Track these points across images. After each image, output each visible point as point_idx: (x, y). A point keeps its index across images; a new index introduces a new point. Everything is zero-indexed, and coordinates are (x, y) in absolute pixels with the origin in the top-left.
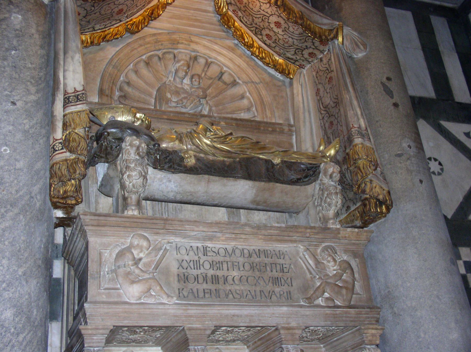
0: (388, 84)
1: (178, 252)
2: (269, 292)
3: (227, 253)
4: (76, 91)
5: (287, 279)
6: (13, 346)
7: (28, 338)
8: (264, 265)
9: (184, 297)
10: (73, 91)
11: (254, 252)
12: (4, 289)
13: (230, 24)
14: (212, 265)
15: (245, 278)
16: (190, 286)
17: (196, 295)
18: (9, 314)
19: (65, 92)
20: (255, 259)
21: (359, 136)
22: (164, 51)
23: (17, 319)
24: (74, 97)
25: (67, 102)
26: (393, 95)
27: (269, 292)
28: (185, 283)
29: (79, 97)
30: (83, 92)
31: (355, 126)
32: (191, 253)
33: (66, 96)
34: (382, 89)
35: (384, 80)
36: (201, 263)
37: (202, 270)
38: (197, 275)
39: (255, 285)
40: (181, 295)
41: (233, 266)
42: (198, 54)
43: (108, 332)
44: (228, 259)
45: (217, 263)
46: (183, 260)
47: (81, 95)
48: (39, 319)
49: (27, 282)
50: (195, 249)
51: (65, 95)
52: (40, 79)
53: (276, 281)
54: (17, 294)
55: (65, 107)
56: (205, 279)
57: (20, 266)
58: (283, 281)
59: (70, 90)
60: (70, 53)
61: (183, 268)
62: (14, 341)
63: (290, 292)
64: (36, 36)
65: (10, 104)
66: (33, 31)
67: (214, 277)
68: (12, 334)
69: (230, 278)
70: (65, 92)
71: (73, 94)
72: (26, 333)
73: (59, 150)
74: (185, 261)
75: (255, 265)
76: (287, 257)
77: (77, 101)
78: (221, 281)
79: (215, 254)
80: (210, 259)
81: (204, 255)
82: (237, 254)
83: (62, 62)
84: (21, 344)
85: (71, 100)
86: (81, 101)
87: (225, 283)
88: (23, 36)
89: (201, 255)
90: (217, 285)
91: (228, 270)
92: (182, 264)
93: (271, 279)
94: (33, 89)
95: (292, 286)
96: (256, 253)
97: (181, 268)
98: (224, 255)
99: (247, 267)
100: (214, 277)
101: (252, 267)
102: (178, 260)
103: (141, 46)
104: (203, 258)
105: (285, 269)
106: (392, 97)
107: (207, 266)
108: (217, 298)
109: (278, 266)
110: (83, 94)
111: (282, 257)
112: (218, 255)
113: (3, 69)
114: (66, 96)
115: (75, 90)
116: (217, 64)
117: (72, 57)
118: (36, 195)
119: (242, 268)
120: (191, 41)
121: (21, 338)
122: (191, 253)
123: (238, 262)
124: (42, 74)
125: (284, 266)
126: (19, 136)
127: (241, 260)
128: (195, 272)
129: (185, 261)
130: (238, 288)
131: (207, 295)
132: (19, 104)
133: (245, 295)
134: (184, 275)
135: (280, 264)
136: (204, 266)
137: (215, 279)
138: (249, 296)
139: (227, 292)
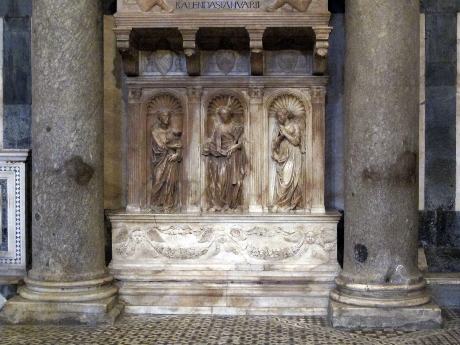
6: (72, 41)
7: (82, 36)
12: (64, 8)
18: (68, 22)
40: (178, 7)
43: (130, 32)
48: (89, 24)
54: (72, 11)
68: (71, 34)
72: (80, 32)
84: (77, 39)
108: (202, 8)
121: (76, 36)
131: (196, 6)
138: (227, 7)
139: (210, 4)
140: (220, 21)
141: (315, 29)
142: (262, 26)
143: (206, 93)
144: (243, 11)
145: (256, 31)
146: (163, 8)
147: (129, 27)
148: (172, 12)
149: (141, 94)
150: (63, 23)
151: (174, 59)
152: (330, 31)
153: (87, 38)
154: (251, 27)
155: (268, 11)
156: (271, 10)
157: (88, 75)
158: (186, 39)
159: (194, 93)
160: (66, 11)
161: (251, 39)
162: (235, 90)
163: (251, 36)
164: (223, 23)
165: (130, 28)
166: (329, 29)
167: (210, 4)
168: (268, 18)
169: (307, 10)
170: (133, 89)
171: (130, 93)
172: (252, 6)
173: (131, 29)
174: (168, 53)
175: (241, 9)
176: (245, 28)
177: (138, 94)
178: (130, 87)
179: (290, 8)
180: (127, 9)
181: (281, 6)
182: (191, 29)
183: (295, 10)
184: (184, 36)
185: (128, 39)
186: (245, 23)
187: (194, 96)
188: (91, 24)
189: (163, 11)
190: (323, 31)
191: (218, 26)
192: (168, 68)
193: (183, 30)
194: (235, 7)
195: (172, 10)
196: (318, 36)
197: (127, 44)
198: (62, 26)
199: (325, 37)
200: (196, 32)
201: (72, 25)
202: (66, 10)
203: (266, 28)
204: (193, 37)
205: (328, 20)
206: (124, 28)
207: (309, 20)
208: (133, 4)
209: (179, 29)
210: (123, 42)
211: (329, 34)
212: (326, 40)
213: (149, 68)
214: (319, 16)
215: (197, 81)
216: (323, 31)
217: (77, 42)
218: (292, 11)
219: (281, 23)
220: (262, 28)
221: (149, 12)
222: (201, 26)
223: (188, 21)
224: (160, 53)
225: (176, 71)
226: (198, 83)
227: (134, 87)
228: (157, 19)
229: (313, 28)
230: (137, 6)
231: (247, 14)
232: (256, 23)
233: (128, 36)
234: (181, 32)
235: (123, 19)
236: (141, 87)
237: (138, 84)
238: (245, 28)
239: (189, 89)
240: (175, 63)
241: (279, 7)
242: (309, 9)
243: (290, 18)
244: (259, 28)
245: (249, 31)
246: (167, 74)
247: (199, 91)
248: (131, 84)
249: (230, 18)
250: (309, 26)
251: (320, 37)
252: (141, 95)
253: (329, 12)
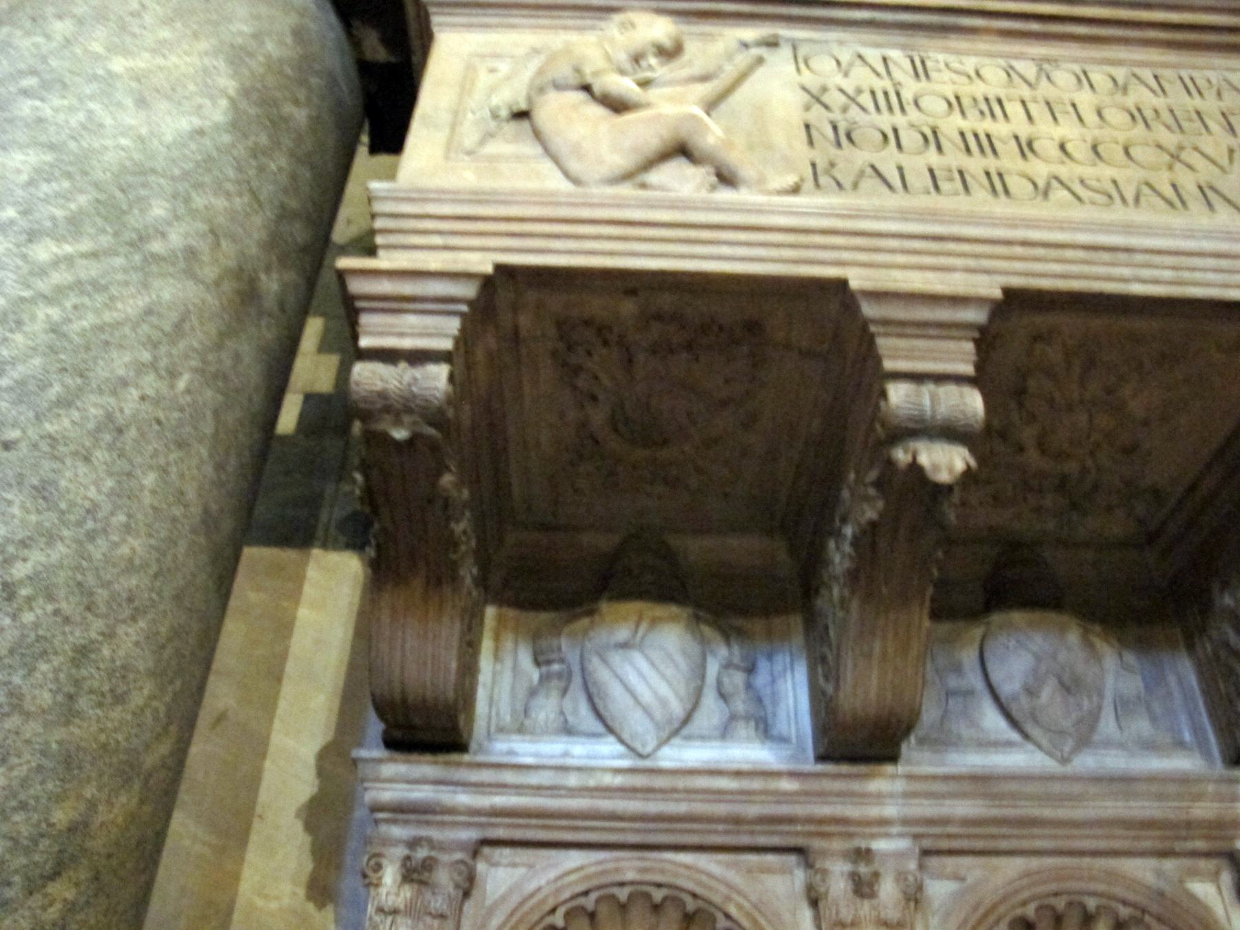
16: (861, 157)
72: (86, 246)
121: (43, 252)
128: (885, 121)
134: (835, 128)
140: (1139, 258)
143: (939, 890)
146: (726, 178)
149: (468, 886)
151: (713, 668)
153: (132, 305)
157: (37, 557)
159: (863, 887)
162: (1142, 870)
164: (1168, 274)
170: (413, 843)
171: (390, 875)
174: (673, 619)
177: (444, 878)
178: (397, 832)
185: (447, 344)
187: (865, 908)
191: (1137, 289)
192: (677, 709)
193: (878, 296)
197: (436, 380)
201: (31, 183)
204: (960, 357)
213: (546, 709)
215: (879, 797)
222: (1016, 282)
223: (917, 245)
224: (618, 623)
225: (725, 733)
226: (890, 810)
227: (423, 832)
234: (869, 310)
236: (469, 835)
237: (452, 811)
239: (824, 853)
240: (719, 684)
246: (666, 751)
247: (901, 877)
248: (402, 811)
252: (467, 894)
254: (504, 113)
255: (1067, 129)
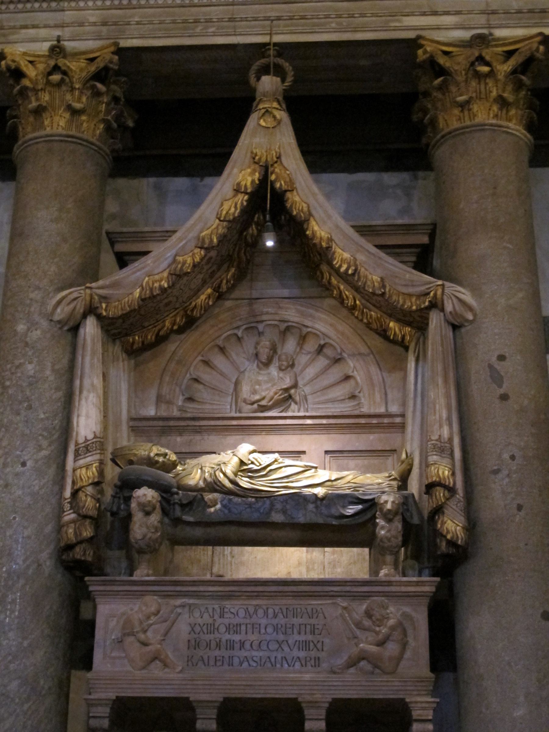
0: (498, 366)
1: (191, 616)
2: (293, 658)
3: (247, 613)
4: (86, 440)
5: (318, 642)
8: (291, 626)
9: (193, 665)
10: (84, 439)
11: (280, 611)
13: (324, 280)
14: (228, 629)
15: (266, 643)
17: (207, 663)
18: (14, 685)
19: (77, 444)
20: (281, 620)
21: (435, 453)
22: (244, 327)
23: (22, 690)
24: (84, 449)
25: (77, 454)
26: (503, 382)
27: (293, 658)
28: (195, 649)
29: (89, 448)
30: (94, 440)
31: (433, 438)
32: (206, 616)
33: (77, 447)
34: (489, 374)
35: (494, 359)
36: (216, 626)
37: (217, 635)
38: (210, 641)
39: (277, 650)
41: (253, 628)
42: (290, 324)
43: (111, 702)
44: (248, 621)
45: (234, 626)
46: (195, 624)
47: (91, 445)
48: (46, 687)
49: (33, 653)
50: (210, 610)
51: (76, 446)
52: (54, 428)
53: (305, 645)
55: (75, 461)
56: (218, 646)
57: (24, 638)
58: (311, 644)
59: (81, 440)
60: (85, 393)
61: (195, 633)
62: (18, 711)
63: (319, 658)
64: (52, 378)
65: (20, 466)
66: (48, 372)
67: (229, 643)
69: (247, 645)
70: (77, 444)
71: (83, 445)
72: (31, 703)
73: (67, 511)
74: (197, 626)
75: (279, 626)
76: (321, 615)
77: (86, 453)
78: (237, 646)
79: (232, 616)
80: (226, 621)
81: (220, 617)
82: (259, 616)
83: (77, 404)
85: (80, 452)
86: (90, 452)
87: (241, 649)
88: (37, 382)
89: (216, 617)
90: (231, 652)
91: (246, 633)
92: (194, 629)
93: (297, 643)
94: (45, 443)
95: (323, 650)
96: (282, 613)
97: (192, 632)
98: (243, 615)
99: (270, 630)
100: (229, 643)
101: (276, 629)
102: (190, 624)
103: (213, 326)
104: (219, 621)
105: (316, 631)
106: (500, 386)
107: (222, 629)
108: (229, 665)
109: (308, 627)
110: (93, 443)
111: (315, 616)
112: (236, 617)
113: (16, 426)
114: (77, 447)
115: (86, 439)
116: (315, 334)
117: (86, 398)
118: (45, 561)
119: (263, 631)
120: (280, 308)
122: (206, 616)
123: (260, 624)
124: (56, 422)
125: (316, 627)
126: (28, 499)
127: (264, 621)
128: (208, 637)
129: (197, 626)
130: (256, 654)
131: (219, 663)
132: (29, 464)
133: (263, 661)
134: (195, 641)
135: (311, 625)
136: (220, 631)
137: (230, 645)
139: (242, 660)
140: (256, 688)
141: (411, 702)
142: (325, 697)
144: (295, 672)
145: (314, 704)
146: (166, 665)
147: (111, 694)
148: (181, 672)
150: (5, 686)
152: (435, 705)
154: (308, 698)
155: (335, 673)
156: (339, 671)
158: (201, 716)
160: (12, 666)
161: (307, 717)
163: (306, 712)
165: (112, 695)
166: (434, 702)
167: (242, 660)
168: (335, 684)
169: (396, 670)
172: (308, 663)
173: (114, 698)
175: (291, 668)
176: (297, 698)
179: (369, 667)
180: (109, 665)
181: (354, 664)
182: (210, 699)
183: (377, 671)
184: (198, 711)
185: (107, 715)
186: (297, 692)
188: (50, 688)
189: (166, 670)
190: (424, 705)
194: (282, 666)
195: (180, 668)
196: (415, 714)
197: (106, 723)
198: (4, 691)
199: (428, 715)
200: (217, 704)
202: (12, 665)
203: (330, 700)
204: (213, 714)
205: (431, 688)
206: (103, 696)
207: (400, 688)
208: (120, 658)
209: (191, 699)
210: (98, 720)
211: (434, 710)
212: (429, 720)
214: (418, 681)
216: (424, 705)
217: (24, 718)
218: (373, 673)
219: (355, 692)
220: (324, 700)
221: (143, 672)
228: (156, 682)
229: (407, 700)
230: (126, 661)
231: (302, 677)
232: (315, 692)
233: (108, 710)
235: (101, 682)
238: (297, 698)
241: (352, 666)
242: (399, 670)
243: (370, 684)
244: (319, 700)
245: (303, 705)
249: (274, 683)
250: (401, 697)
251: (418, 715)
253: (432, 675)
254: (116, 641)
255: (253, 637)
